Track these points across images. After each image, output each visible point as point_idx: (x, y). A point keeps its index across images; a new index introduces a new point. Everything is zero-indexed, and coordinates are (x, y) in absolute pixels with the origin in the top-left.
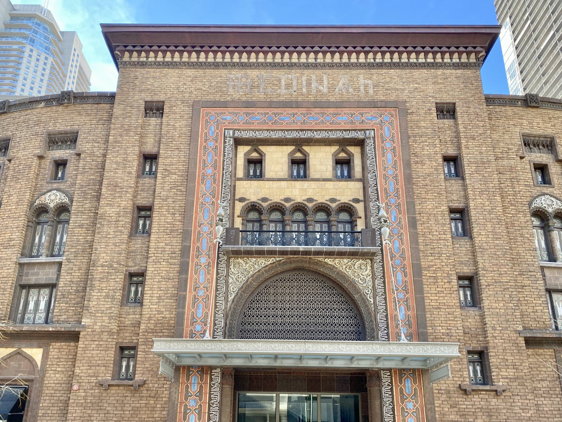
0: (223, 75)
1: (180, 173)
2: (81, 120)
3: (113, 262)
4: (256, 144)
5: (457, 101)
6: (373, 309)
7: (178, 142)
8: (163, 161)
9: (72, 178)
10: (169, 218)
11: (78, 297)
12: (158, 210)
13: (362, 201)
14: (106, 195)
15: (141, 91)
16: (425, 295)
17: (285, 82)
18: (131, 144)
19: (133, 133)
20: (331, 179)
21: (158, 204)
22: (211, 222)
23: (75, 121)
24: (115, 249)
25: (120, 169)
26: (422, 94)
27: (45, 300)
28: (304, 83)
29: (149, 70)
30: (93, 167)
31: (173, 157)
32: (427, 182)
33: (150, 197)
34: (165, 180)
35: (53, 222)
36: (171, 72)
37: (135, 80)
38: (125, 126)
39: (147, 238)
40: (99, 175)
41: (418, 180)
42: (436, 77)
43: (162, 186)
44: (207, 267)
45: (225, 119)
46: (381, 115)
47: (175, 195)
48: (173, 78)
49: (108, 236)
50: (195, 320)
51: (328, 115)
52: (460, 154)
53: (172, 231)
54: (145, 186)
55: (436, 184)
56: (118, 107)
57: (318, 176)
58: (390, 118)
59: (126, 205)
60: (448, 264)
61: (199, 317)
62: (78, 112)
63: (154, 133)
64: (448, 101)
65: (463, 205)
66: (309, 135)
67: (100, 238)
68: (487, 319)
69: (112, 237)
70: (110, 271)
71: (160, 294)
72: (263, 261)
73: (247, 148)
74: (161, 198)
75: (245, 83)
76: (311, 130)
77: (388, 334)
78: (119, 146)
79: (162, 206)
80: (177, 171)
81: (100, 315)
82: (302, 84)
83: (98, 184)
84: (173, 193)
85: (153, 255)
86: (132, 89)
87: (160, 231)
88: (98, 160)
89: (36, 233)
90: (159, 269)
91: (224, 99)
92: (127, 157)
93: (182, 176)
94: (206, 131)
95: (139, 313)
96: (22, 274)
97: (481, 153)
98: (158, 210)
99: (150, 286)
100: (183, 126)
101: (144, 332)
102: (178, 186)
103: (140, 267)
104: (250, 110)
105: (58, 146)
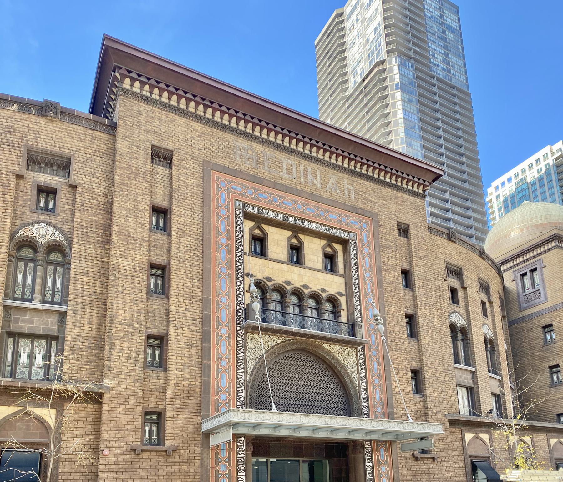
0: (230, 140)
1: (195, 237)
2: (73, 143)
3: (133, 321)
4: (259, 222)
5: (411, 223)
6: (358, 391)
7: (190, 202)
8: (177, 219)
9: (65, 213)
10: (187, 282)
11: (91, 355)
12: (175, 272)
13: (344, 295)
14: (118, 244)
15: (147, 131)
16: (392, 382)
17: (286, 166)
18: (141, 191)
19: (142, 178)
20: (322, 270)
21: (175, 265)
22: (228, 294)
23: (65, 143)
24: (133, 307)
25: (130, 217)
26: (388, 210)
27: (41, 353)
28: (302, 172)
29: (154, 108)
30: (94, 207)
31: (186, 216)
32: (392, 288)
33: (164, 255)
34: (181, 241)
35: (44, 261)
36: (177, 119)
37: (139, 115)
38: (132, 168)
39: (165, 300)
40: (102, 217)
41: (386, 285)
42: (397, 198)
43: (178, 246)
44: (227, 338)
45: (235, 189)
46: (361, 221)
47: (191, 259)
48: (180, 127)
49: (125, 292)
50: (220, 390)
51: (322, 210)
52: (411, 269)
53: (191, 297)
54: (158, 242)
55: (398, 292)
56: (122, 143)
57: (311, 265)
58: (367, 227)
59: (141, 260)
60: (405, 359)
61: (223, 387)
62: (68, 133)
63: (163, 184)
64: (405, 222)
65: (412, 312)
66: (306, 225)
67: (116, 292)
68: (428, 405)
69: (129, 294)
70: (130, 330)
71: (184, 360)
72: (275, 339)
73: (251, 224)
74: (178, 259)
75: (251, 156)
76: (309, 221)
77: (368, 412)
78: (128, 190)
79: (179, 269)
80: (192, 233)
81: (123, 377)
82: (300, 173)
83: (101, 228)
84: (190, 256)
85: (174, 319)
86: (136, 125)
87: (180, 294)
88: (99, 199)
89: (18, 271)
90: (181, 335)
91: (232, 167)
92: (137, 205)
93: (197, 239)
94: (217, 196)
95: (162, 378)
96: (9, 319)
97: (425, 272)
98: (175, 272)
99: (173, 351)
100: (195, 185)
101: (171, 398)
102: (193, 250)
103: (159, 330)
104: (258, 186)
105: (41, 168)
